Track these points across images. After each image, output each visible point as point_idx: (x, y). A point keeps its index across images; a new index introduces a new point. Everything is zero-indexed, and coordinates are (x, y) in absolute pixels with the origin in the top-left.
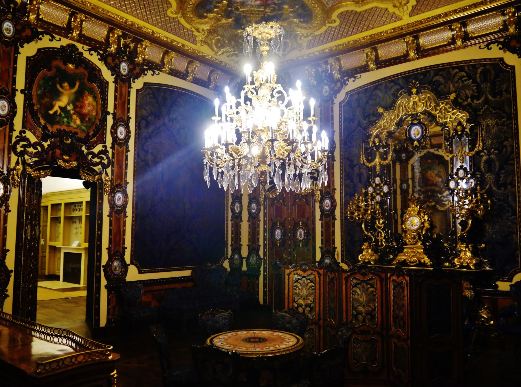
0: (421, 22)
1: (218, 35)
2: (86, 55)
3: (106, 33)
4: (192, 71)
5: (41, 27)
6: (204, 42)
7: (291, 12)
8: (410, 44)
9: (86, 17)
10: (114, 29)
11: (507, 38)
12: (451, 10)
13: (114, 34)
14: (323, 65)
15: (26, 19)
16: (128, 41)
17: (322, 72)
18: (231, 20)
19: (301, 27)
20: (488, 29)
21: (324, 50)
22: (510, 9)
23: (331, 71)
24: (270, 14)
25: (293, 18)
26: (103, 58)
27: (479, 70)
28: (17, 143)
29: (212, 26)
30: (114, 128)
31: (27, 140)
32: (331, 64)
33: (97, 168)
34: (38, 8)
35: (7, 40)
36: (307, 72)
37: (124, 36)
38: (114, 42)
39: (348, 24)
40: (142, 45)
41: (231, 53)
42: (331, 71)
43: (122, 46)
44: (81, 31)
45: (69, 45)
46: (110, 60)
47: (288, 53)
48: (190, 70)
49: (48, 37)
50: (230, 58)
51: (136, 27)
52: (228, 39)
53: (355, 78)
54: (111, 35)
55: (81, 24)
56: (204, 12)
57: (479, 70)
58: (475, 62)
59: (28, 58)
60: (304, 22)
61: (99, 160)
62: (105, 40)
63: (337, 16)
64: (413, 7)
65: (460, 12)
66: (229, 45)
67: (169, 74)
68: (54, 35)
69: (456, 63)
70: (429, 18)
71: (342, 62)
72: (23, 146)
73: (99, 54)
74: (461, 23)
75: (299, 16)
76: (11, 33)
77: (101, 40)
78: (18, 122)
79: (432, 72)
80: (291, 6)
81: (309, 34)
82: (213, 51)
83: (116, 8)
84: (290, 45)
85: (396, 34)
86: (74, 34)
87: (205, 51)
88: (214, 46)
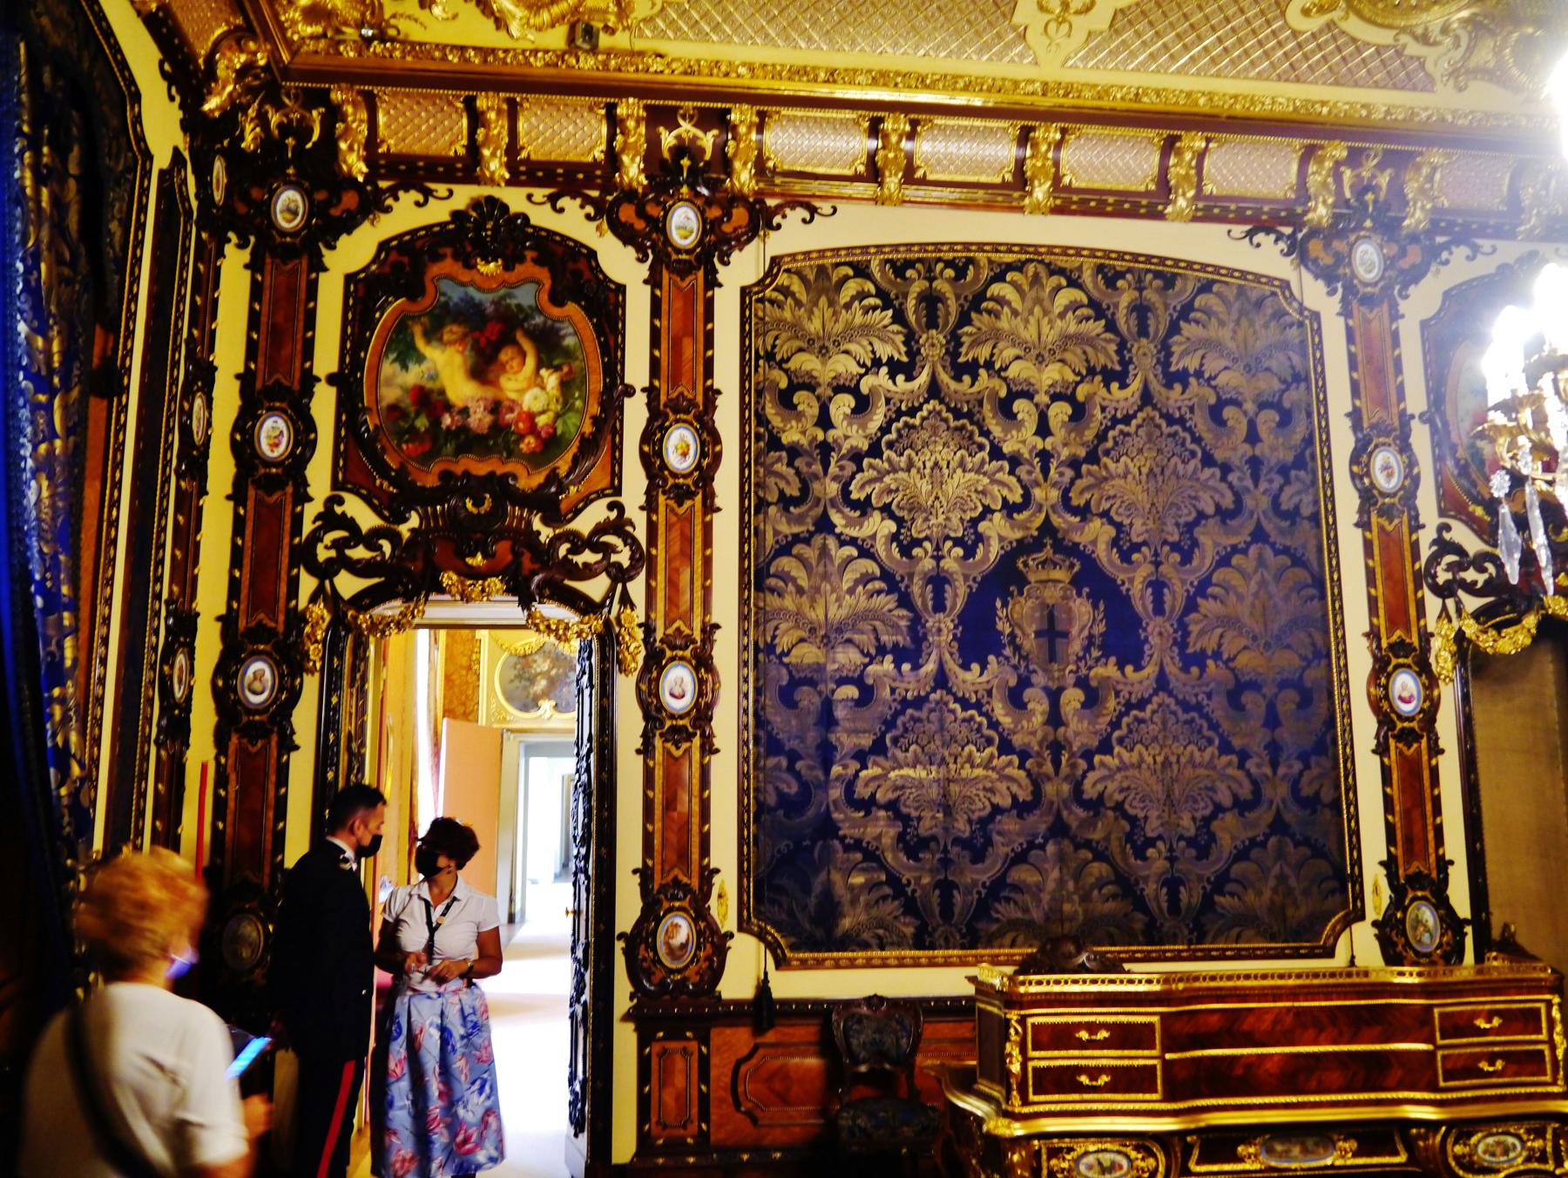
2: (542, 217)
26: (604, 212)
28: (315, 537)
30: (653, 437)
31: (349, 523)
33: (596, 587)
45: (476, 204)
46: (627, 213)
49: (415, 195)
59: (349, 278)
61: (599, 556)
68: (432, 186)
72: (338, 545)
73: (587, 200)
78: (319, 475)
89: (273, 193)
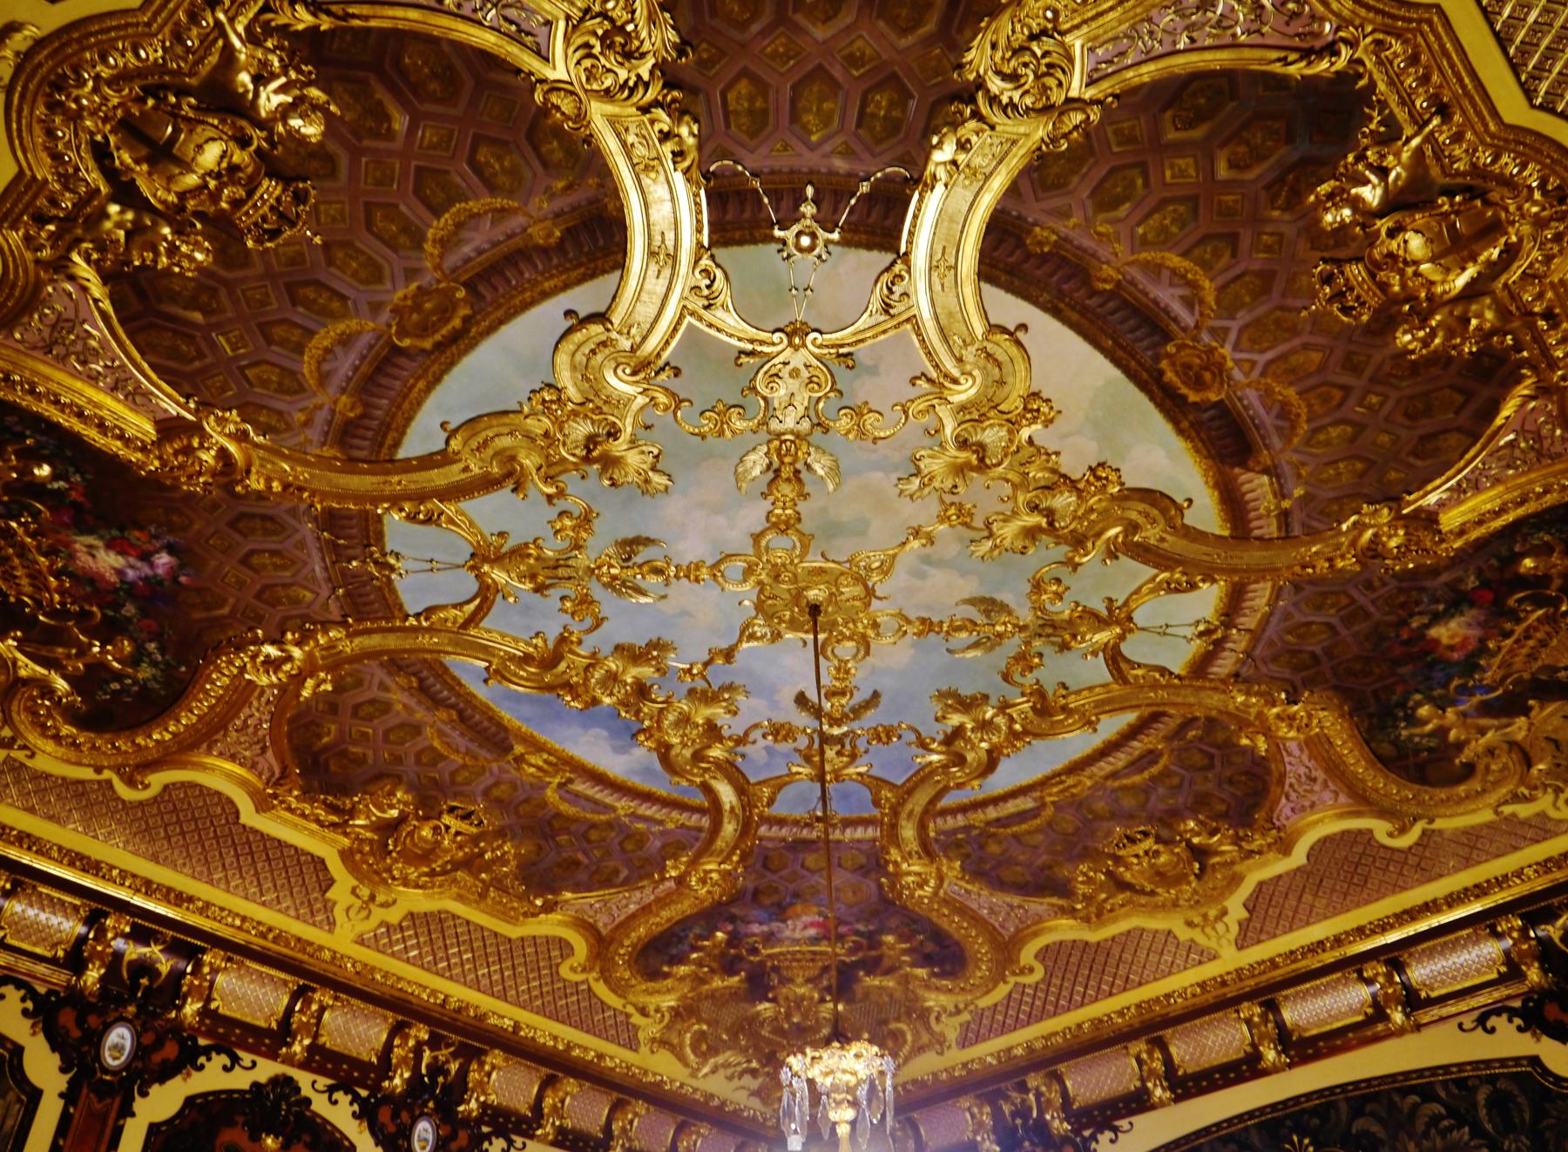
0: (1273, 963)
1: (699, 1021)
2: (320, 1105)
3: (384, 1037)
4: (624, 1130)
5: (208, 1034)
6: (663, 1043)
7: (905, 952)
8: (1257, 1026)
9: (336, 998)
10: (409, 1026)
11: (1531, 999)
12: (1348, 927)
13: (406, 1038)
14: (1014, 1094)
15: (173, 1015)
16: (443, 1054)
17: (1014, 1115)
18: (736, 979)
19: (937, 989)
20: (1466, 975)
21: (1009, 1050)
22: (1508, 921)
23: (1041, 1112)
24: (847, 960)
25: (914, 965)
26: (366, 1113)
27: (1482, 1097)
29: (684, 997)
32: (1037, 1089)
34: (212, 983)
35: (108, 1078)
36: (968, 1115)
37: (435, 1042)
38: (404, 1060)
39: (1069, 976)
40: (482, 1064)
41: (739, 1069)
42: (1041, 1112)
43: (424, 1071)
44: (316, 1036)
45: (277, 1081)
46: (384, 1115)
47: (906, 1060)
48: (616, 1127)
49: (224, 1060)
50: (736, 1083)
51: (472, 1013)
52: (728, 1031)
53: (1116, 1130)
54: (397, 1042)
55: (319, 1017)
56: (663, 963)
57: (1482, 1097)
58: (1460, 1071)
60: (942, 975)
62: (379, 1059)
63: (1036, 957)
64: (1240, 924)
65: (1373, 932)
66: (732, 1045)
67: (555, 1144)
68: (240, 1053)
69: (1407, 1075)
70: (1292, 952)
71: (1069, 1084)
73: (356, 1098)
74: (1387, 963)
75: (926, 960)
76: (123, 1059)
77: (366, 1059)
79: (1343, 1107)
80: (902, 938)
81: (961, 1006)
82: (686, 1064)
83: (422, 967)
84: (909, 1037)
85: (1209, 998)
86: (297, 1048)
87: (663, 1067)
88: (688, 1050)
89: (107, 1027)
